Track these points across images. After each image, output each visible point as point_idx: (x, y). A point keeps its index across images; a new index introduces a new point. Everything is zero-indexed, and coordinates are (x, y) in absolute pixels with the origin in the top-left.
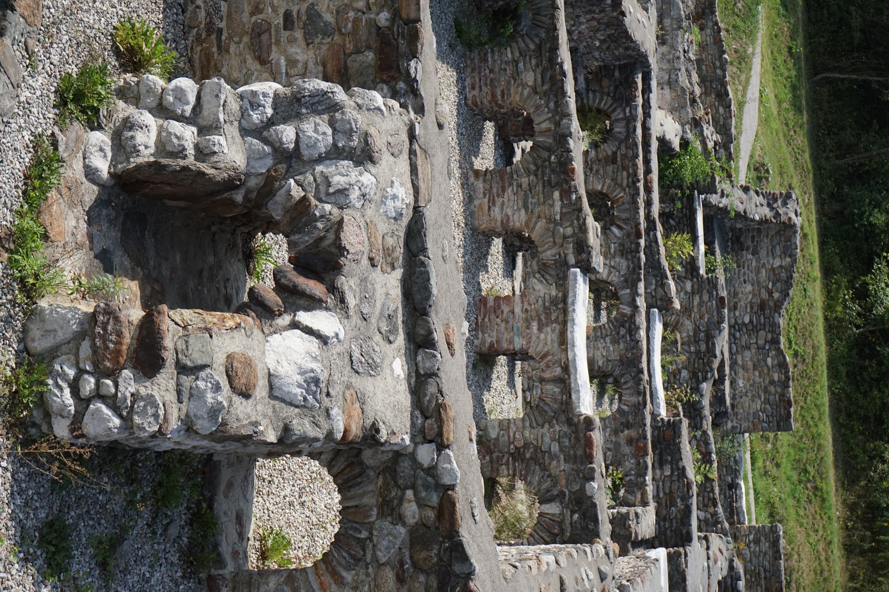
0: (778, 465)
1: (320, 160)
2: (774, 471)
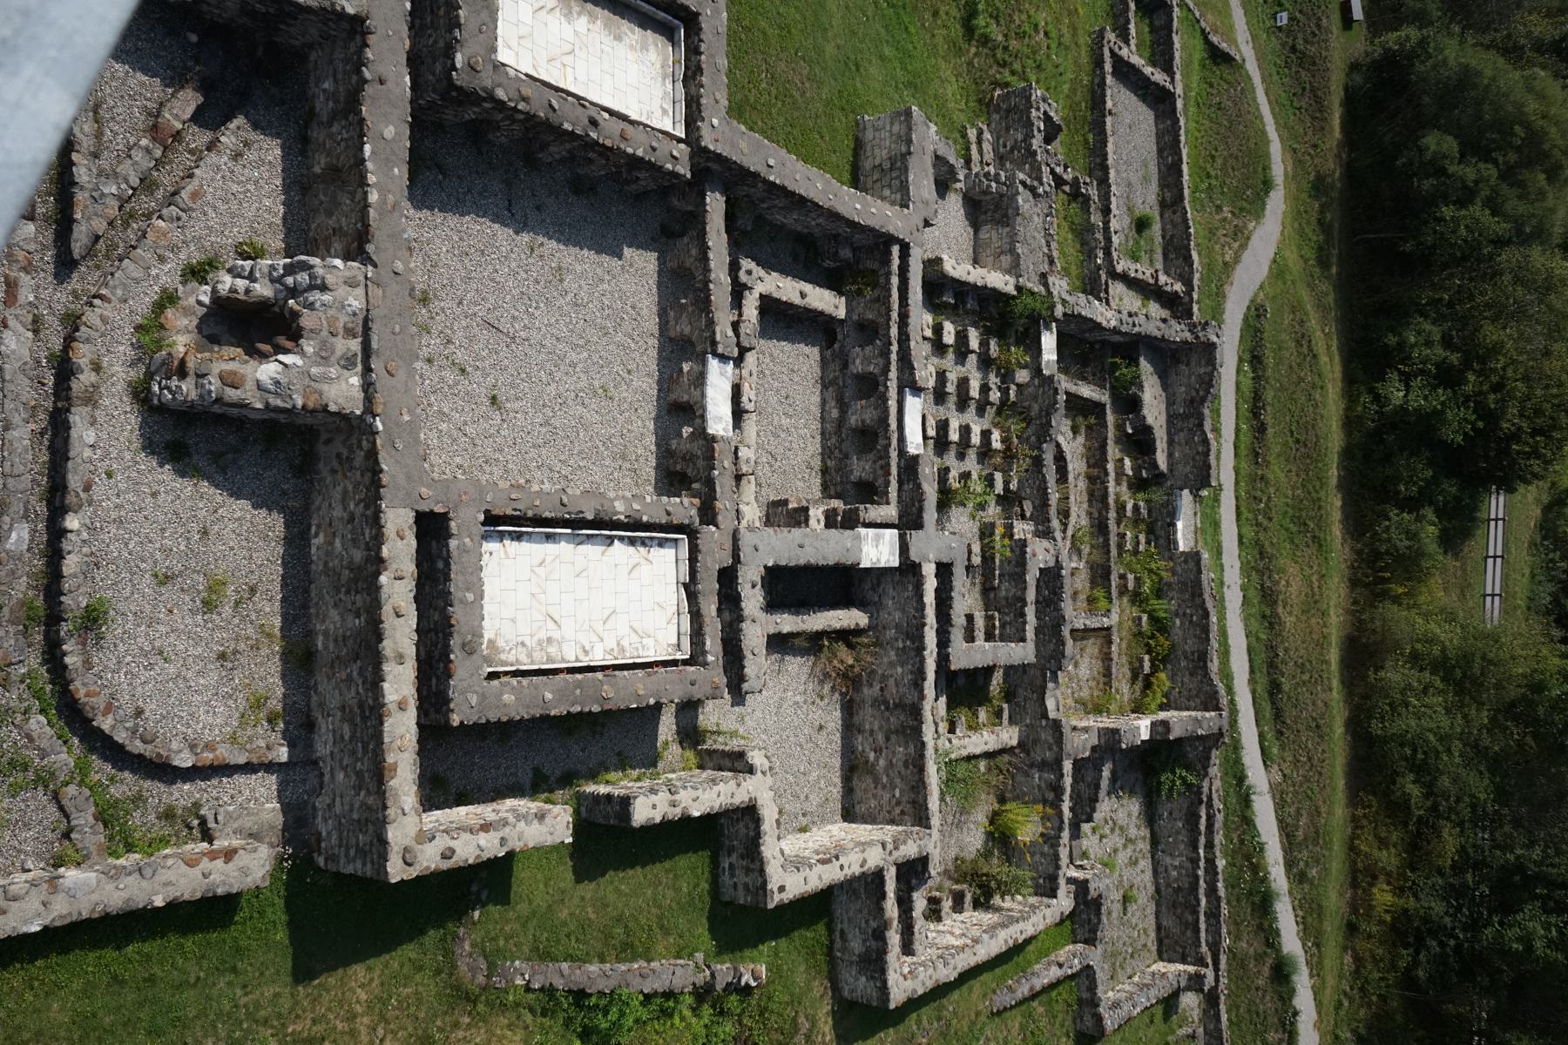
0: (1270, 519)
1: (306, 291)
2: (1265, 522)
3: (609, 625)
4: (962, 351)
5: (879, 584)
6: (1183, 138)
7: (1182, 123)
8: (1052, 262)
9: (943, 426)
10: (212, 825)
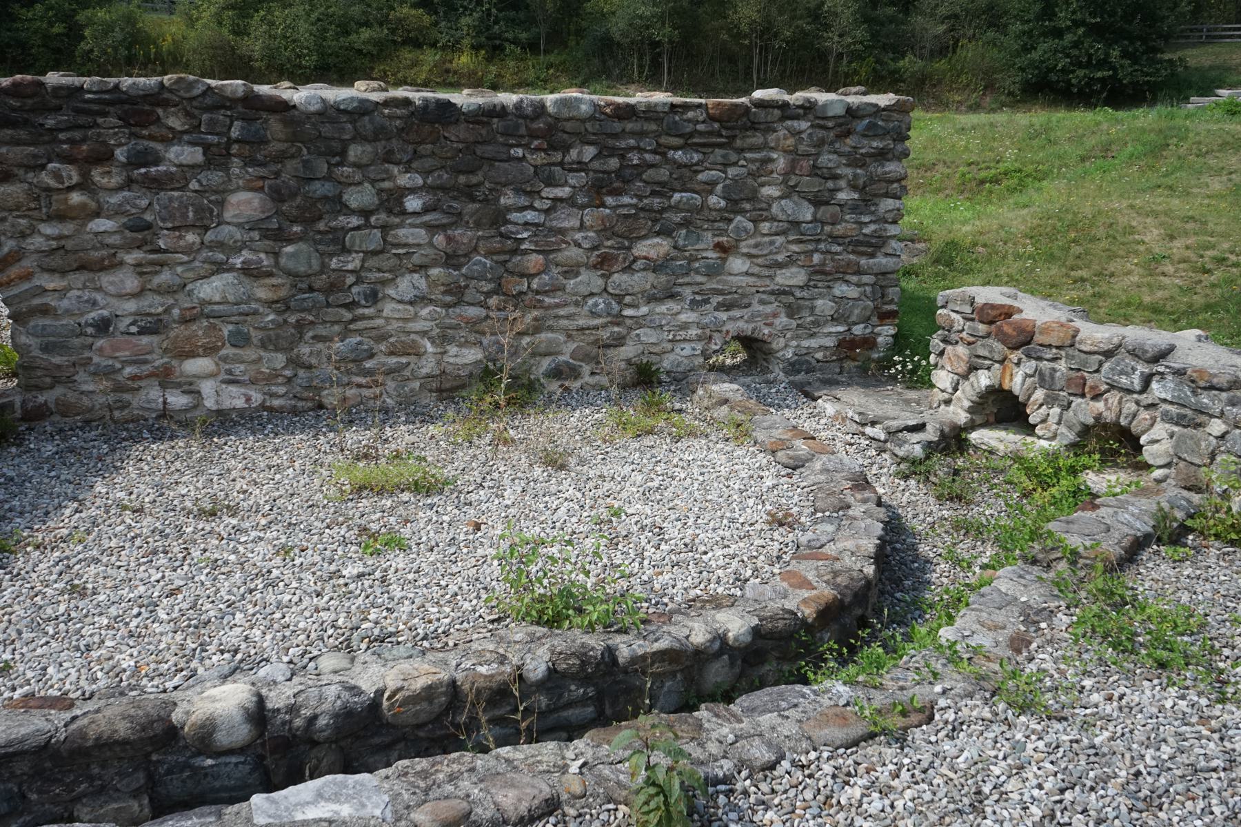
10: (931, 434)
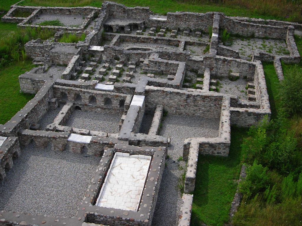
3: (135, 177)
4: (91, 73)
5: (150, 103)
6: (53, 8)
7: (48, 7)
8: (74, 45)
9: (111, 80)
